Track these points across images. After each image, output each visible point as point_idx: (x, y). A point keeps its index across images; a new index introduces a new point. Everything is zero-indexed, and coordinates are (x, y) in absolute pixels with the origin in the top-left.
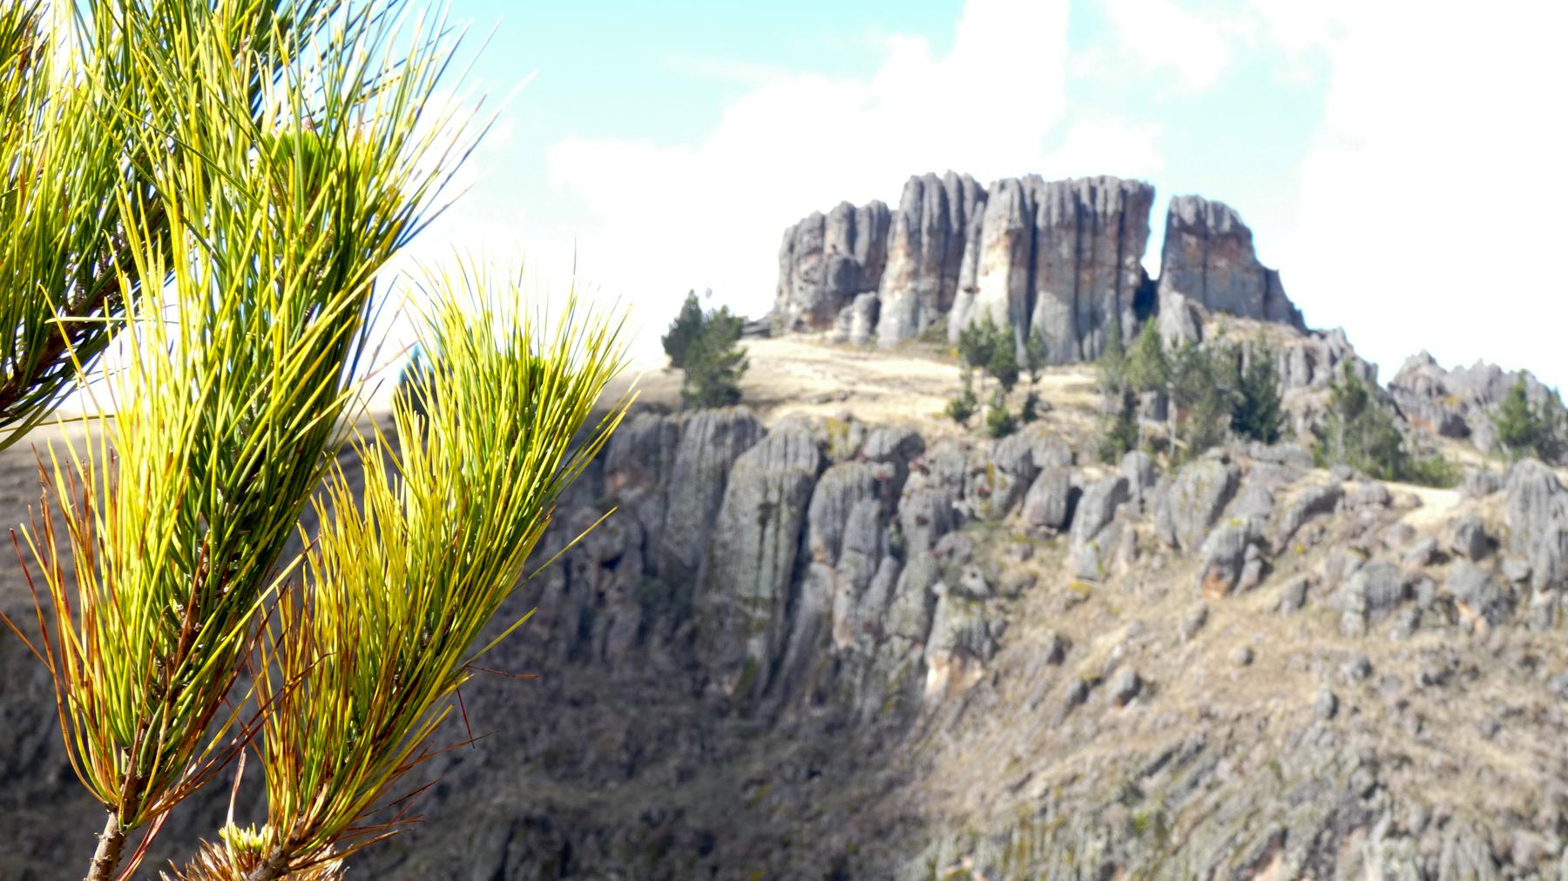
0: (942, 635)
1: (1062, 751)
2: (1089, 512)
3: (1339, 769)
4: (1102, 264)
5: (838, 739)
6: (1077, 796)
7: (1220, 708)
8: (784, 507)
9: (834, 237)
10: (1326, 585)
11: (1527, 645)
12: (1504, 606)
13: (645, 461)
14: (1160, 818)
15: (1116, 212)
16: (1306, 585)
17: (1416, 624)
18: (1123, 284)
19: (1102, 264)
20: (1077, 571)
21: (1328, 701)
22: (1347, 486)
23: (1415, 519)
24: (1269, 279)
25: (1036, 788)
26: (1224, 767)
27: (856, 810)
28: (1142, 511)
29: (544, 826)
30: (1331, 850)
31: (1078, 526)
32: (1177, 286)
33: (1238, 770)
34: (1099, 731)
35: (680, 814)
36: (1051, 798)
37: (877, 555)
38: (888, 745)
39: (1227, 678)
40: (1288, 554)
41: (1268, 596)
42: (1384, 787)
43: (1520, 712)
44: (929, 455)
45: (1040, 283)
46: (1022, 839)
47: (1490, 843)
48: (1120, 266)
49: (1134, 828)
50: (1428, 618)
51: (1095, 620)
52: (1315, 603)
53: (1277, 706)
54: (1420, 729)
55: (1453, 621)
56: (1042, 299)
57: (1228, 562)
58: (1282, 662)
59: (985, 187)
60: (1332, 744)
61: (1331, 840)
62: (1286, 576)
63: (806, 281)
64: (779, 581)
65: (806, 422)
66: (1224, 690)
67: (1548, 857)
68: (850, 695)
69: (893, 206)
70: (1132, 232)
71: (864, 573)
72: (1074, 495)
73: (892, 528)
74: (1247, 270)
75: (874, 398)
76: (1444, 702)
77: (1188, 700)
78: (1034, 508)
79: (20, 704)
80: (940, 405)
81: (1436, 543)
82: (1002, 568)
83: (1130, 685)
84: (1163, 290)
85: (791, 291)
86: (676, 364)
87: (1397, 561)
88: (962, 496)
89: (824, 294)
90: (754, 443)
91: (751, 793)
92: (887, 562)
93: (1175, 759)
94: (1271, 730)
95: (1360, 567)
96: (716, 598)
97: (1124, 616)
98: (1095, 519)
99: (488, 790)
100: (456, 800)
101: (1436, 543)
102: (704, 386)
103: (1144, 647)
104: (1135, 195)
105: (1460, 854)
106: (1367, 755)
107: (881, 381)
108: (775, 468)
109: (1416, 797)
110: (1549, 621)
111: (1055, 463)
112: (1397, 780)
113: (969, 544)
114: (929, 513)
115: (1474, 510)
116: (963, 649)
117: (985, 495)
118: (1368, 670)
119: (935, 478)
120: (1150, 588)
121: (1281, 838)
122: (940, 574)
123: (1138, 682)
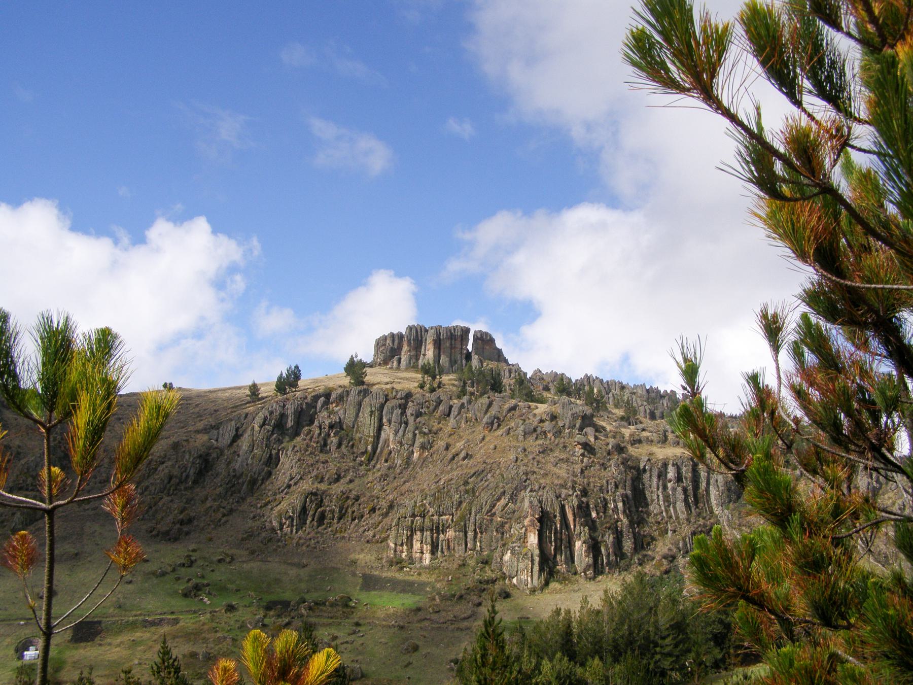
0: (417, 444)
1: (448, 472)
2: (455, 411)
5: (391, 471)
7: (488, 461)
9: (389, 341)
12: (558, 433)
13: (340, 400)
14: (473, 489)
16: (509, 429)
17: (537, 438)
23: (536, 411)
24: (499, 352)
26: (489, 475)
29: (315, 494)
30: (516, 496)
31: (452, 415)
32: (476, 354)
33: (493, 476)
35: (350, 491)
37: (401, 424)
38: (404, 472)
41: (500, 432)
43: (563, 459)
44: (414, 397)
48: (462, 348)
49: (467, 492)
50: (540, 437)
55: (546, 437)
65: (382, 389)
67: (570, 495)
68: (394, 460)
69: (404, 333)
72: (451, 407)
75: (399, 383)
80: (416, 384)
84: (473, 354)
86: (348, 375)
88: (422, 408)
91: (369, 485)
96: (358, 435)
98: (456, 413)
100: (293, 488)
107: (401, 379)
108: (374, 401)
112: (533, 478)
114: (414, 412)
116: (423, 447)
117: (428, 408)
119: (415, 403)
120: (470, 431)
122: (417, 428)
123: (467, 454)
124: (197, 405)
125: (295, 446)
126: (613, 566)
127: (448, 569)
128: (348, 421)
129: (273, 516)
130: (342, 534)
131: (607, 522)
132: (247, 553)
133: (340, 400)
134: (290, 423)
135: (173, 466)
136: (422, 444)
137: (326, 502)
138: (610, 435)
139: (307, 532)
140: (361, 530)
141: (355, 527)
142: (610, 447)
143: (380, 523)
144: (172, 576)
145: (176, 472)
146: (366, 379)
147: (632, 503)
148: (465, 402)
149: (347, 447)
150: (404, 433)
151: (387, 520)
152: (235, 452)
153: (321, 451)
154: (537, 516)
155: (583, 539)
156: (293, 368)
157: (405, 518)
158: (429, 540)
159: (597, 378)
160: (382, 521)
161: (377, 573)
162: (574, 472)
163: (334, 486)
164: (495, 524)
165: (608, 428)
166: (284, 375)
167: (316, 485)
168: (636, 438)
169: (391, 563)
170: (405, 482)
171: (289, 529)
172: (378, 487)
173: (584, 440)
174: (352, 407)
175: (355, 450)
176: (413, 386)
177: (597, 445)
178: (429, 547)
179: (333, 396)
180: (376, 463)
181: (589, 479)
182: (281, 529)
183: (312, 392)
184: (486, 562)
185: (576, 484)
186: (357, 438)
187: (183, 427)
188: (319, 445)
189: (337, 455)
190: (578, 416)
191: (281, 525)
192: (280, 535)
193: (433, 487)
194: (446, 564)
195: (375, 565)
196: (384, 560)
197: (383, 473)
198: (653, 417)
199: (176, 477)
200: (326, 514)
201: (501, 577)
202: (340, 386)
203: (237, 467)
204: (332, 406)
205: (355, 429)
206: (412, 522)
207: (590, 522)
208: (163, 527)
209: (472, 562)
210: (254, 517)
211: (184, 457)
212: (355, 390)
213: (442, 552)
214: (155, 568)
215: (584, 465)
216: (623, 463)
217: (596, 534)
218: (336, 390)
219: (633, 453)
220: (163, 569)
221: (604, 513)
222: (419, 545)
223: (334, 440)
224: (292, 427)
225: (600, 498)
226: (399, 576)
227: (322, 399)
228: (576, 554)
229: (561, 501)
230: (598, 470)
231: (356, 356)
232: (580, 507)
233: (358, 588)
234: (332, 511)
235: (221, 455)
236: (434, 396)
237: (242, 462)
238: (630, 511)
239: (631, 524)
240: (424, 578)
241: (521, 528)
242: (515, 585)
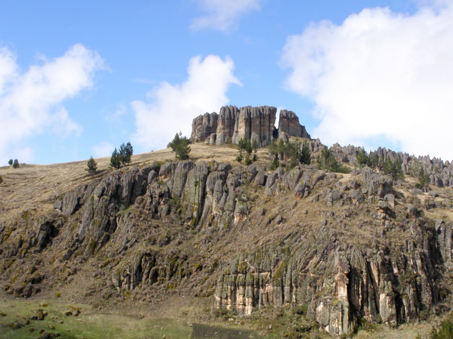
0: (237, 210)
1: (266, 235)
2: (269, 181)
3: (328, 236)
4: (266, 126)
5: (215, 234)
6: (270, 245)
7: (301, 224)
8: (200, 182)
9: (205, 121)
10: (323, 196)
11: (368, 207)
12: (362, 199)
13: (168, 172)
14: (289, 249)
15: (268, 114)
16: (319, 196)
17: (343, 204)
18: (270, 130)
19: (266, 126)
20: (267, 194)
21: (325, 222)
22: (326, 174)
23: (340, 180)
24: (303, 128)
25: (261, 243)
26: (303, 237)
27: (220, 249)
28: (281, 180)
29: (149, 255)
30: (326, 254)
31: (267, 184)
32: (282, 130)
33: (306, 237)
34: (274, 230)
35: (180, 251)
36: (264, 245)
37: (222, 192)
38: (226, 235)
39: (302, 217)
40: (314, 189)
41: (310, 199)
42: (338, 240)
43: (367, 222)
44: (233, 169)
45: (252, 130)
46: (258, 255)
47: (362, 251)
48: (270, 126)
49: (283, 251)
50: (346, 202)
51: (271, 205)
52: (321, 200)
53: (314, 223)
54: (345, 227)
55: (351, 203)
56: (253, 133)
57: (301, 191)
58: (314, 213)
59: (239, 109)
60: (326, 231)
61: (327, 252)
62: (314, 194)
63: (199, 131)
64: (200, 199)
65: (204, 162)
66: (302, 220)
67: (374, 254)
68: (217, 224)
69: (218, 113)
70: (272, 119)
71: (219, 197)
72: (266, 178)
73: (225, 186)
74: (298, 126)
75: (219, 157)
76: (350, 221)
77: (294, 222)
78: (257, 181)
79: (31, 231)
80: (234, 158)
81: (347, 185)
82: (250, 194)
83: (280, 219)
84: (279, 131)
85: (195, 133)
86: (174, 150)
87: (338, 190)
88: (240, 178)
89: (203, 134)
90: (193, 168)
91: (195, 246)
92: (224, 194)
93: (291, 236)
94: (312, 228)
95: (330, 192)
96: (185, 203)
97: (278, 204)
98: (271, 183)
99: (136, 247)
100: (129, 250)
101: (347, 185)
102: (181, 155)
103: (283, 211)
104: (272, 110)
105: (355, 254)
106: (334, 233)
107: (219, 153)
108: (198, 173)
109: (345, 242)
110: (372, 202)
111: (261, 170)
112: (341, 238)
113: (243, 189)
114: (233, 183)
115: (355, 178)
116: (242, 213)
117: (246, 178)
118: (333, 214)
119: (234, 174)
120: (284, 198)
121: (316, 252)
122: (237, 196)
123: (282, 219)
124: (41, 179)
125: (130, 214)
126: (414, 316)
127: (267, 318)
128: (176, 191)
129: (113, 274)
130: (173, 290)
131: (407, 278)
132: (90, 307)
133: (168, 172)
134: (125, 193)
135: (24, 232)
136: (241, 209)
137: (158, 261)
138: (407, 200)
139: (143, 287)
140: (190, 285)
141: (184, 283)
142: (408, 211)
143: (206, 279)
144: (28, 328)
145: (26, 237)
146: (191, 154)
147: (429, 260)
148: (278, 172)
149: (175, 213)
150: (226, 200)
151: (213, 277)
152: (77, 219)
153: (153, 217)
154: (346, 272)
155: (387, 292)
156: (126, 145)
157: (229, 274)
158: (250, 293)
159: (390, 151)
160: (208, 278)
161: (205, 323)
162: (377, 233)
163: (165, 248)
164: (308, 279)
165: (406, 194)
166: (118, 151)
167: (150, 247)
168: (431, 203)
169: (217, 314)
170: (227, 244)
171: (127, 285)
172: (203, 248)
173: (385, 205)
174: (179, 179)
175: (183, 216)
176: (231, 159)
177: (396, 209)
178: (251, 300)
179: (162, 169)
180: (201, 227)
181: (390, 239)
182: (120, 286)
183: (142, 166)
184: (301, 313)
185: (379, 243)
186: (184, 205)
187: (31, 198)
188: (151, 212)
189: (166, 221)
190: (380, 184)
191: (120, 282)
192: (119, 290)
193: (252, 247)
194: (266, 314)
195: (203, 316)
196: (211, 312)
197: (208, 235)
198: (441, 184)
199: (26, 242)
200: (159, 272)
201: (315, 325)
202: (167, 161)
203: (79, 233)
204: (161, 178)
205: (182, 198)
206: (235, 278)
207: (392, 278)
208: (17, 285)
209: (289, 313)
210: (96, 276)
211: (33, 224)
212: (181, 164)
213: (262, 304)
214: (12, 322)
215: (385, 227)
216: (420, 225)
217: (398, 287)
218: (164, 164)
219: (428, 216)
220: (19, 322)
221: (405, 269)
222: (241, 298)
223: (163, 207)
224: (127, 196)
225: (401, 256)
226: (225, 325)
227: (153, 172)
228: (381, 305)
229: (366, 259)
230: (398, 231)
231: (181, 134)
232: (383, 264)
233: (190, 336)
234: (164, 270)
235: (65, 222)
236: (250, 168)
237: (84, 228)
238: (427, 268)
239: (429, 278)
240: (247, 327)
241: (332, 283)
242: (327, 333)
